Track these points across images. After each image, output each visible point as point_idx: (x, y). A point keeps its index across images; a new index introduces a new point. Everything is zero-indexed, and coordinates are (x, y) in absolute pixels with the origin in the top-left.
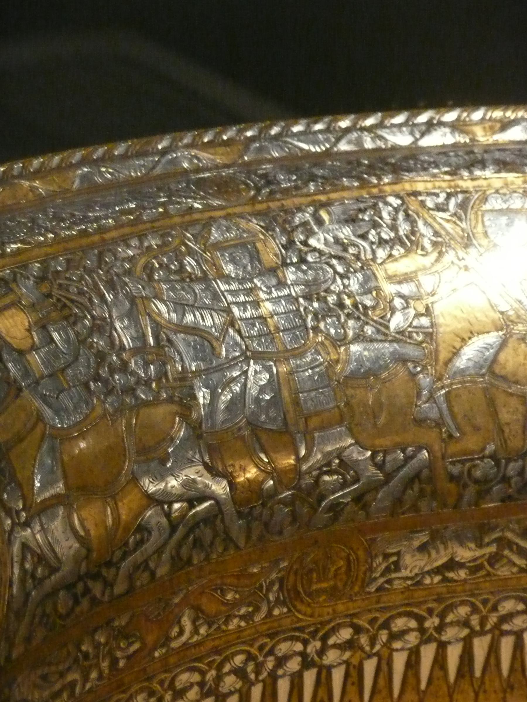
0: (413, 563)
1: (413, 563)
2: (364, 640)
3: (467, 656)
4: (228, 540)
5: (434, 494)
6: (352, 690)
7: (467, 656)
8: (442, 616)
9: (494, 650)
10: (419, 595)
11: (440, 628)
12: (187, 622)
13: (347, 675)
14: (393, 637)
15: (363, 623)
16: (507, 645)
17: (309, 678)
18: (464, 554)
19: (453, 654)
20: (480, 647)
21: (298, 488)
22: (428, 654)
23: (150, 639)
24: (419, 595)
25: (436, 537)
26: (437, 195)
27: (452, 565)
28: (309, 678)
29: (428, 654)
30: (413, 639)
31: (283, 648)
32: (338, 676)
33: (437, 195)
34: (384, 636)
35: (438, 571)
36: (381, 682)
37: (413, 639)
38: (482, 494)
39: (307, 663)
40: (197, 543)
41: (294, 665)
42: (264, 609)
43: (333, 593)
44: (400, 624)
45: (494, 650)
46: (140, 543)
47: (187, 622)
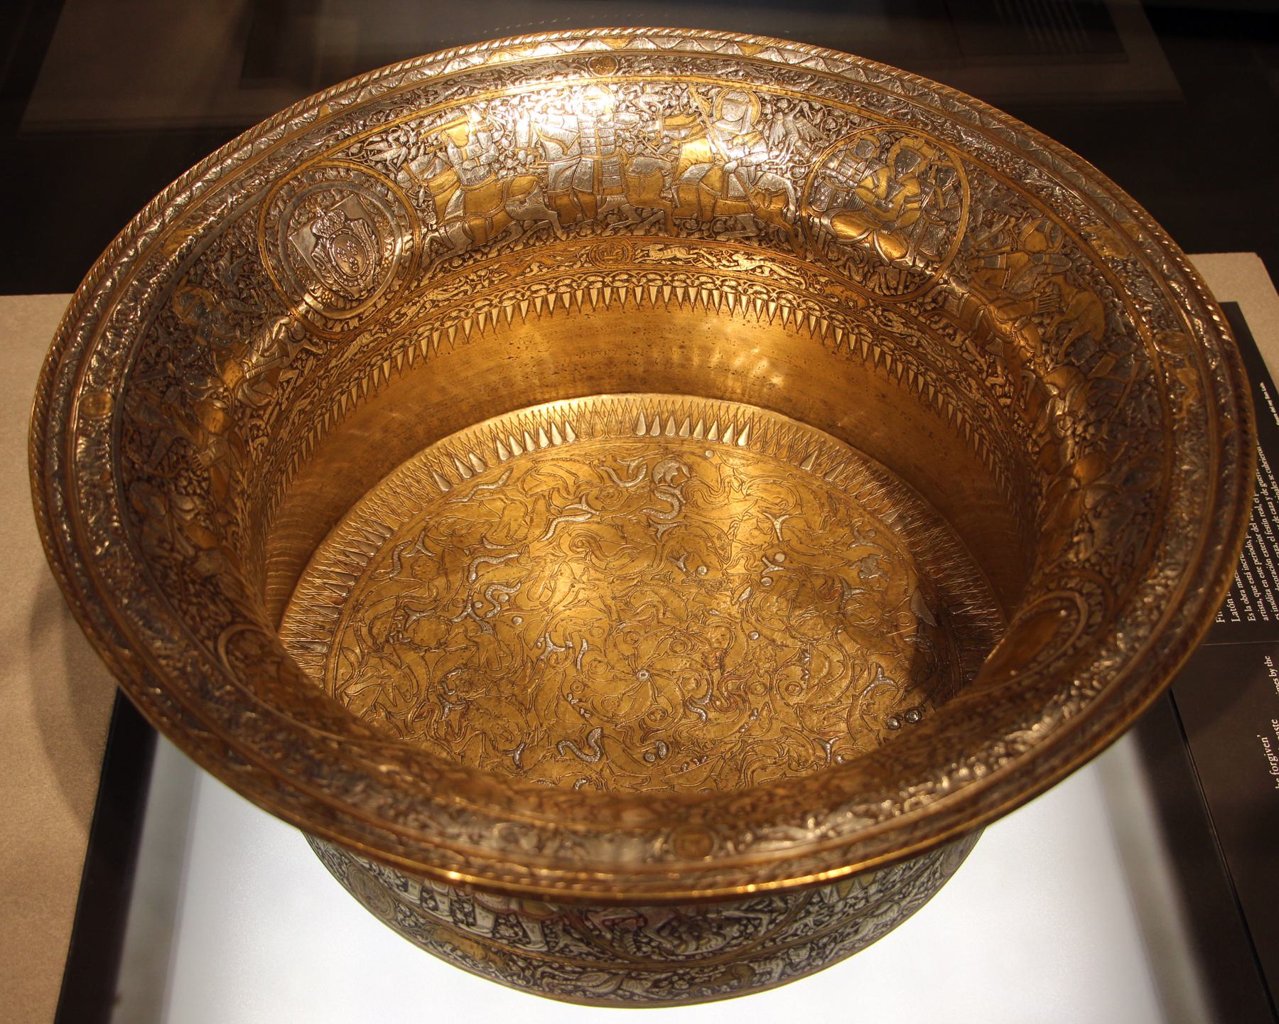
0: (655, 255)
1: (655, 255)
2: (634, 280)
3: (686, 294)
4: (556, 238)
5: (666, 231)
6: (631, 298)
7: (686, 294)
8: (673, 277)
9: (699, 293)
10: (660, 267)
11: (672, 281)
12: (535, 267)
13: (627, 292)
14: (649, 281)
15: (633, 273)
16: (705, 294)
17: (608, 291)
18: (679, 256)
19: (680, 292)
20: (692, 292)
21: (595, 219)
22: (667, 290)
23: (513, 274)
24: (660, 267)
25: (667, 247)
26: (183, 404)
27: (675, 259)
28: (608, 291)
29: (667, 290)
30: (659, 283)
31: (592, 279)
32: (622, 292)
33: (183, 404)
34: (644, 280)
35: (669, 260)
36: (645, 296)
37: (659, 283)
38: (689, 234)
39: (605, 285)
40: (539, 239)
41: (599, 285)
42: (579, 264)
43: (616, 261)
44: (651, 276)
45: (699, 293)
46: (503, 238)
47: (535, 267)
